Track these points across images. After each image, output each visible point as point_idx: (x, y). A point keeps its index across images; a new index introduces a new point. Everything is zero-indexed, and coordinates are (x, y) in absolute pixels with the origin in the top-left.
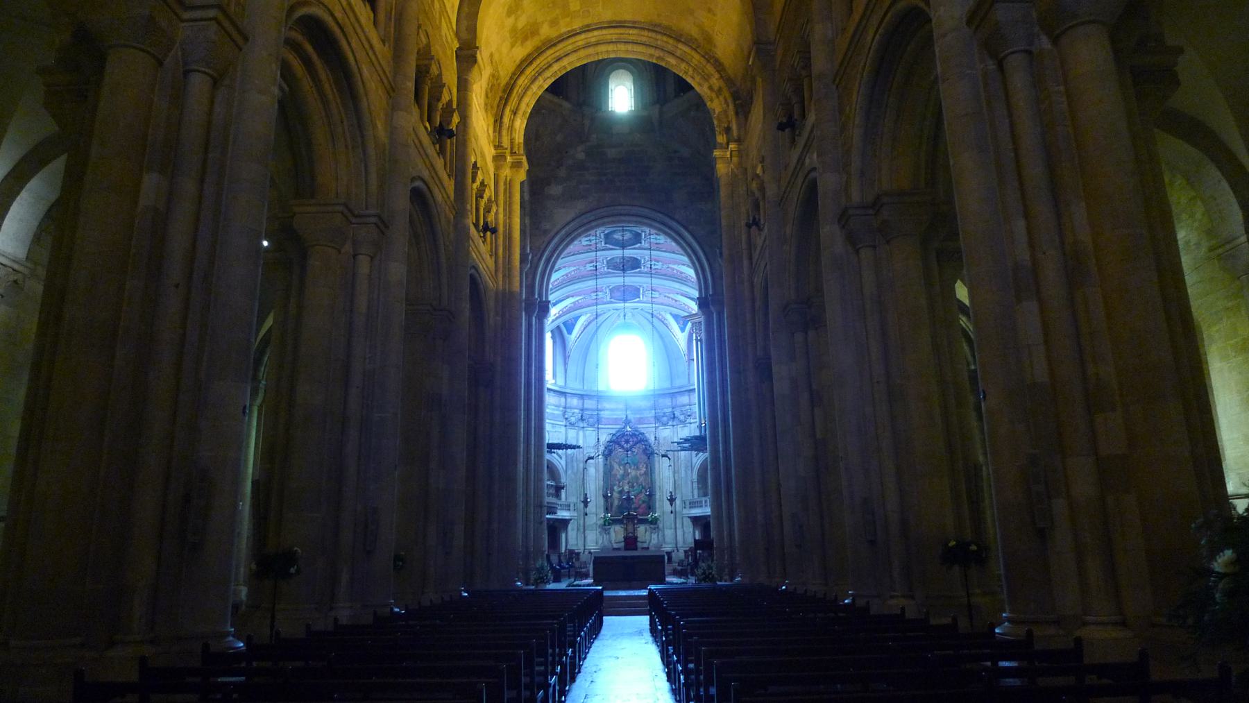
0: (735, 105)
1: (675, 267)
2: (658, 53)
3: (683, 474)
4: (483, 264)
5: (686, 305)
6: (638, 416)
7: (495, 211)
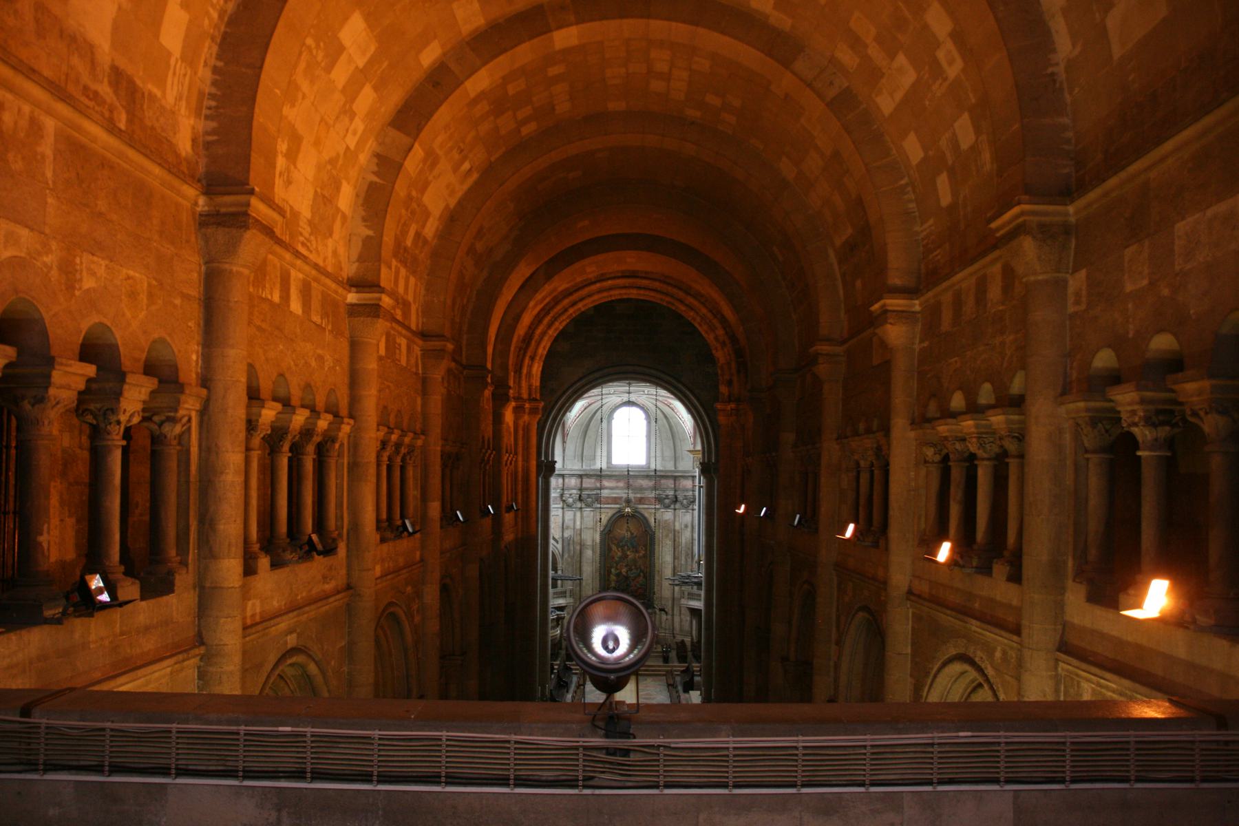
2: (668, 299)
3: (683, 562)
6: (639, 496)
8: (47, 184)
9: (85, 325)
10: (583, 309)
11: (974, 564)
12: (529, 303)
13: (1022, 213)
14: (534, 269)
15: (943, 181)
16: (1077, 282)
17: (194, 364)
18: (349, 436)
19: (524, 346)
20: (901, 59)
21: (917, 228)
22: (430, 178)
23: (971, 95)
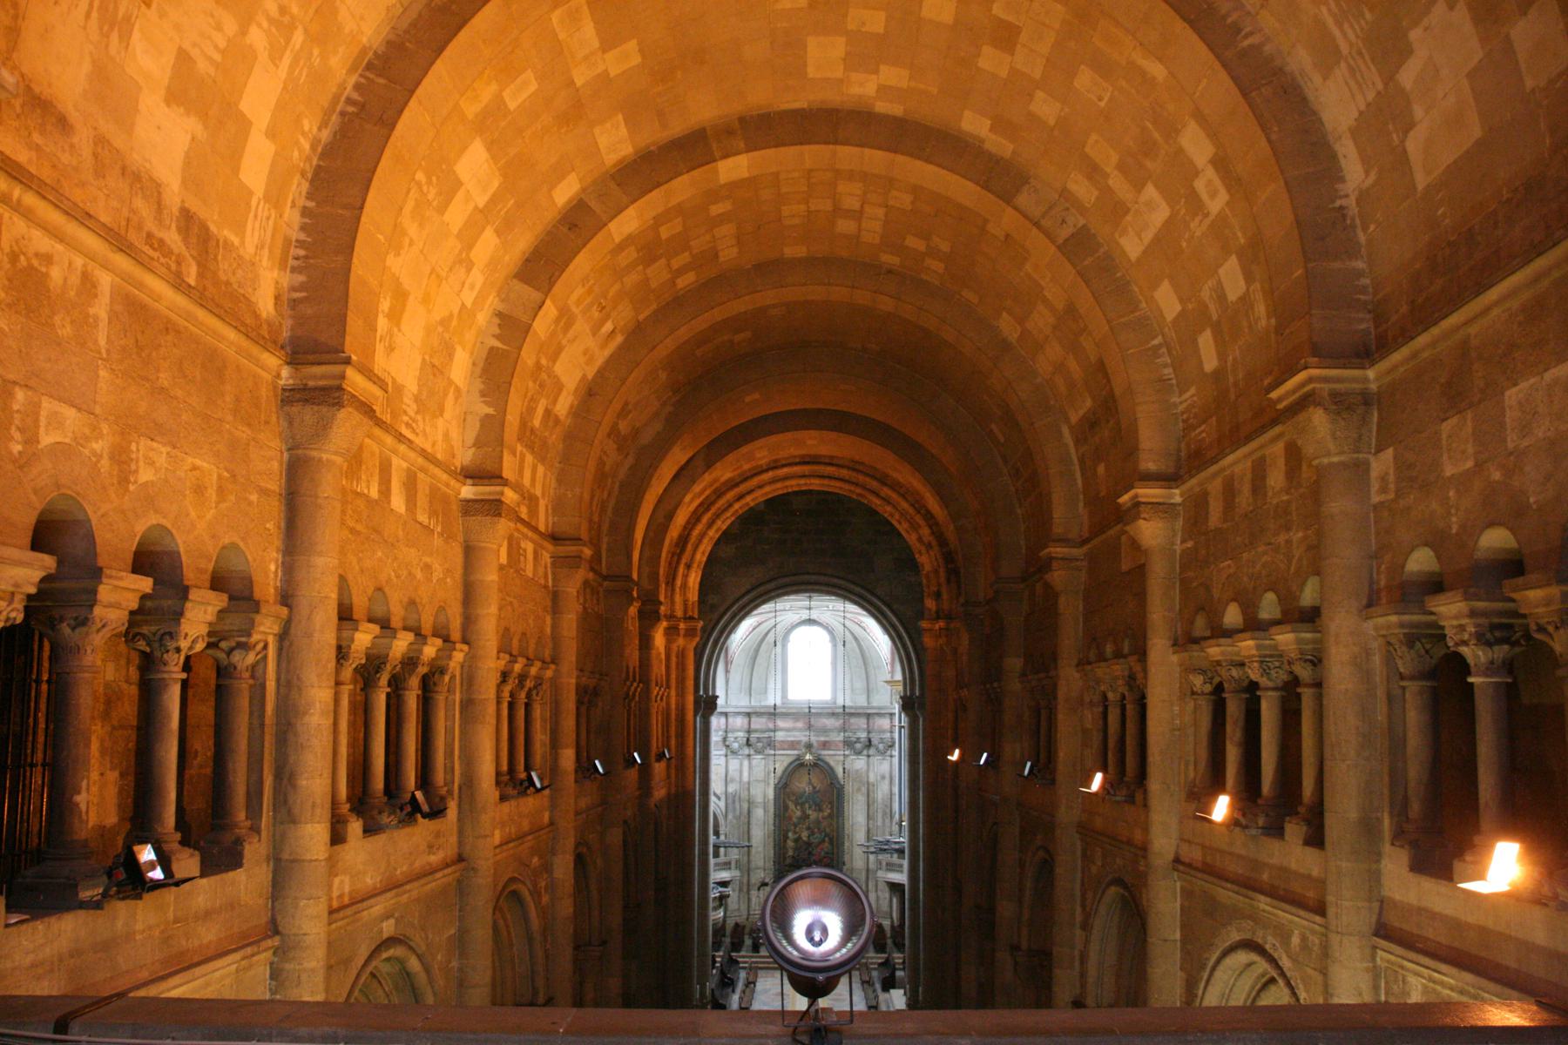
2: (859, 491)
3: (880, 823)
6: (822, 739)
8: (100, 353)
9: (140, 528)
10: (752, 504)
11: (1261, 821)
12: (684, 496)
13: (1310, 380)
14: (691, 454)
15: (1206, 341)
16: (1382, 464)
17: (272, 576)
18: (462, 667)
20: (1150, 192)
21: (1175, 399)
22: (564, 342)
23: (1239, 234)
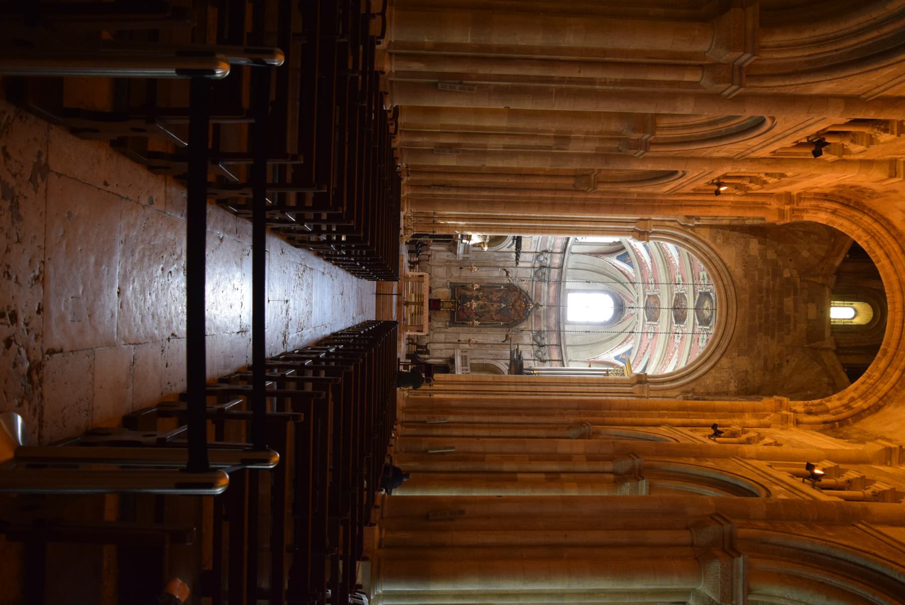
0: (833, 422)
1: (676, 355)
2: (891, 350)
4: (687, 183)
5: (639, 362)
6: (542, 315)
7: (738, 193)
19: (851, 205)
